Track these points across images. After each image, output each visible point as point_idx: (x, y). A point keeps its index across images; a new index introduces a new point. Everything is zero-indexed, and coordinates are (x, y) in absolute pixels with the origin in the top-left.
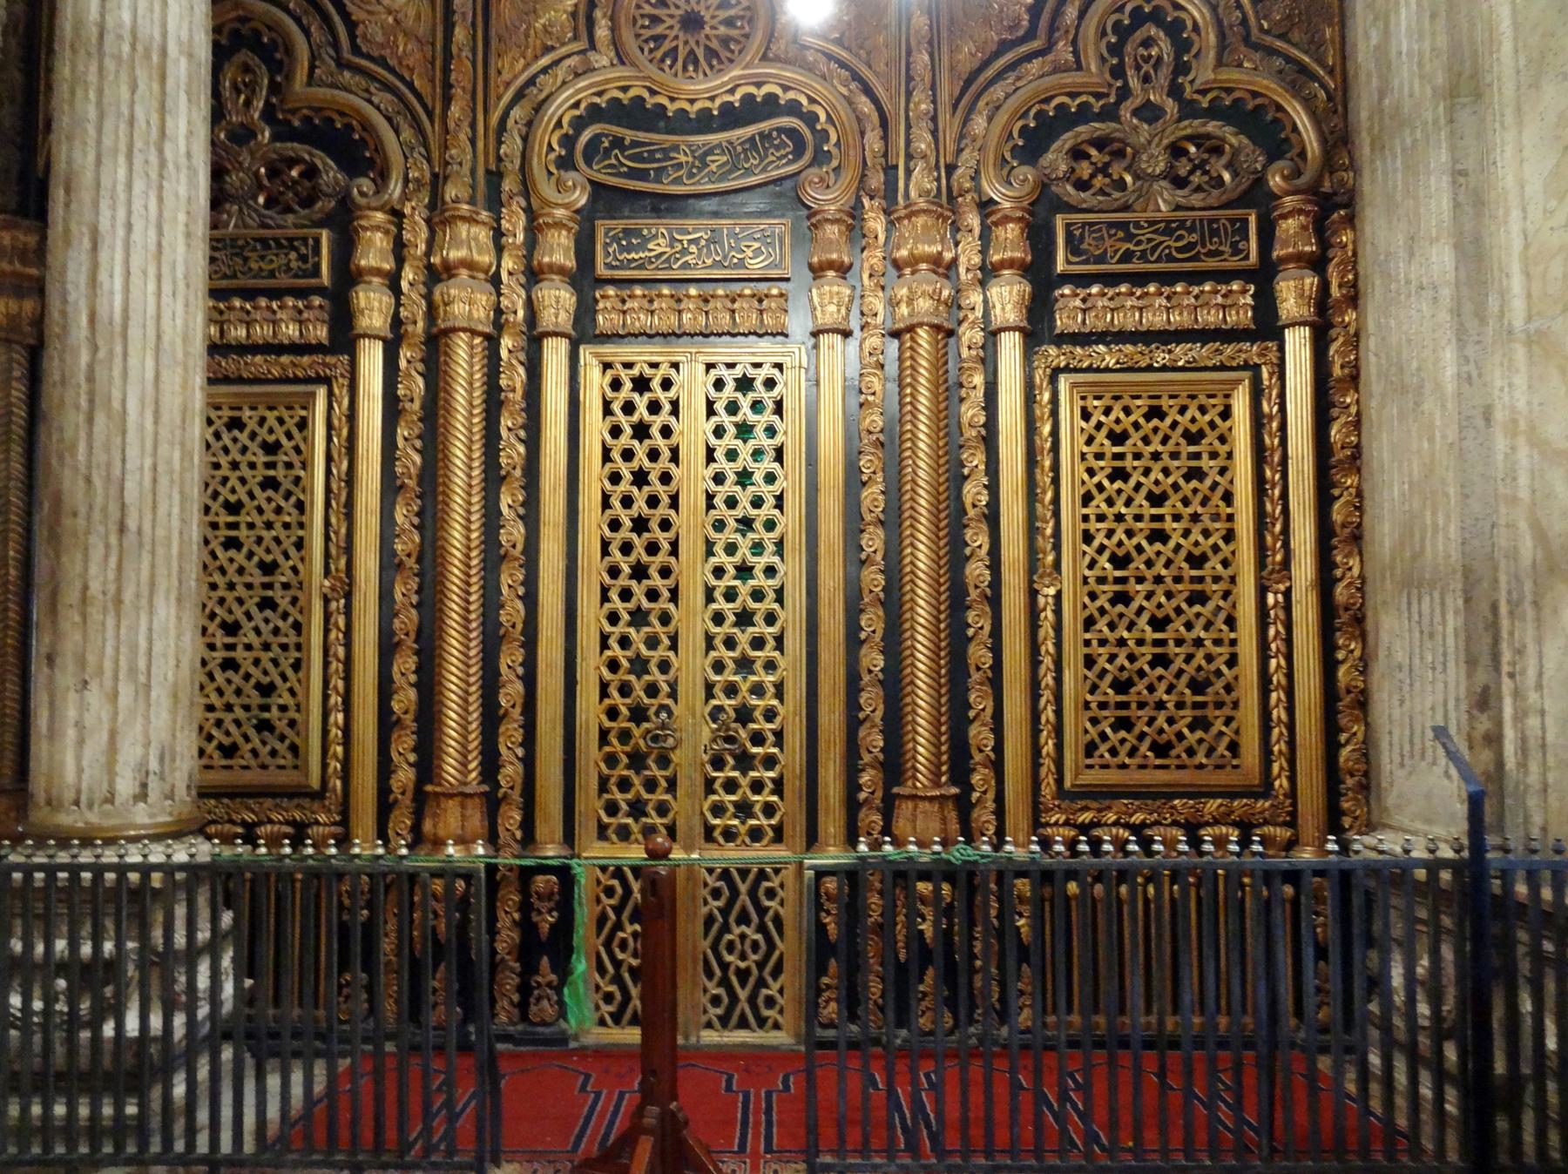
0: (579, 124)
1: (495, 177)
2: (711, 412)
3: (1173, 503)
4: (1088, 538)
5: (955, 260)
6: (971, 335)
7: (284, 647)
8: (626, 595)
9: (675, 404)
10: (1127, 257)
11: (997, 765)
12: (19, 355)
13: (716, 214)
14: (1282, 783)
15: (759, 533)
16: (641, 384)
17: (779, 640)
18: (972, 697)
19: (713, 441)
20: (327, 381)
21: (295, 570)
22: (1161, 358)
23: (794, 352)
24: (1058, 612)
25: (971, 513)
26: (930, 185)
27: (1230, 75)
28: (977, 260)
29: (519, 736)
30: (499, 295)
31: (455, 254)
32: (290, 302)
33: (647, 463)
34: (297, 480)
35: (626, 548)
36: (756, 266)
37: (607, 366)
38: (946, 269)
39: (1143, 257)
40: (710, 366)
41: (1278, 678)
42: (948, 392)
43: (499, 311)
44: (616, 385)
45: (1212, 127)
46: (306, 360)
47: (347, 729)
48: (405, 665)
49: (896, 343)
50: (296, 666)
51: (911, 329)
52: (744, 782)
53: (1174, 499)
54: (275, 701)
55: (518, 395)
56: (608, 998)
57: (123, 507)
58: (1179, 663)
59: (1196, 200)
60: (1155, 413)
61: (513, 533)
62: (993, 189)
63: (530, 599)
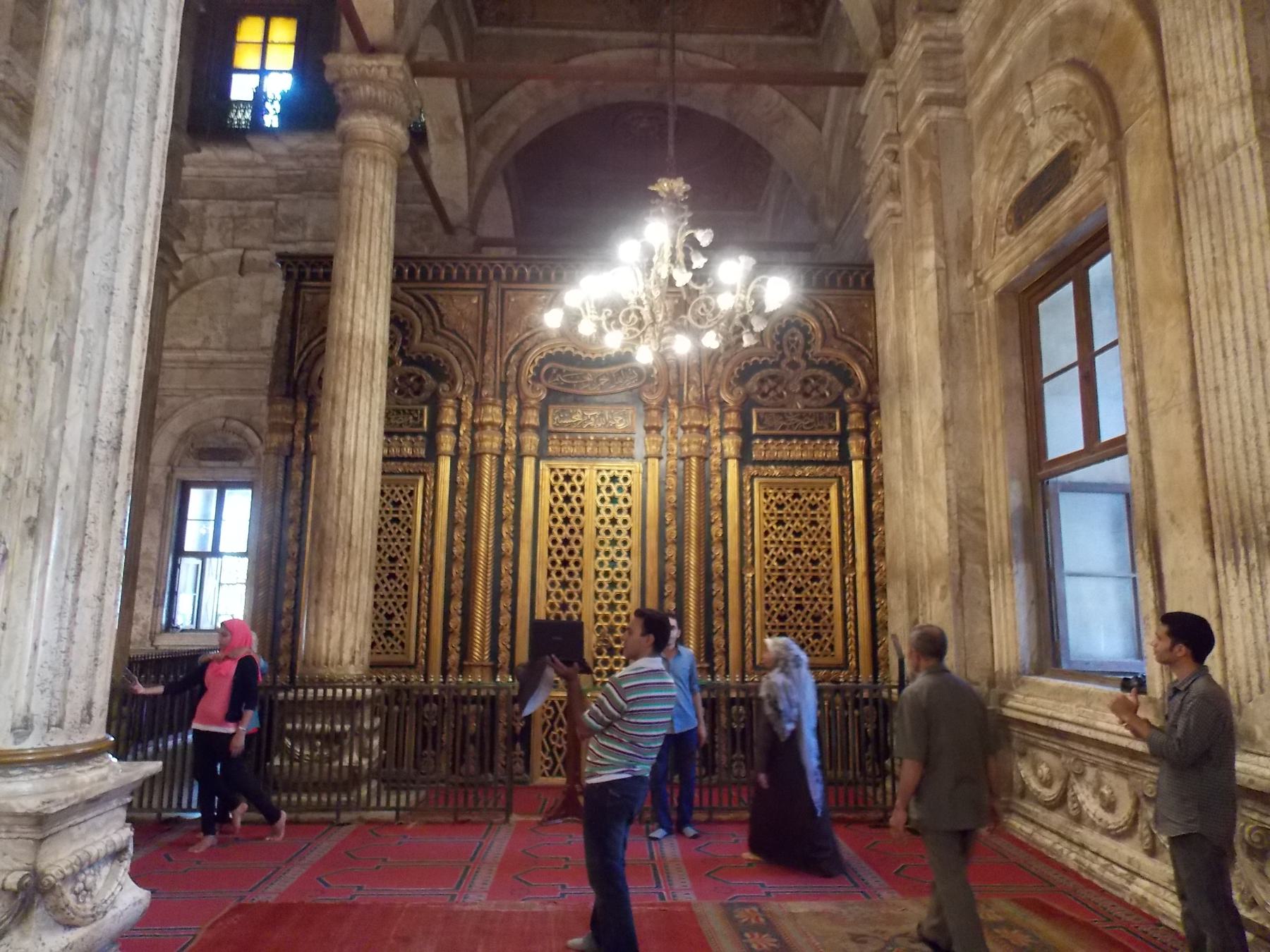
0: (542, 362)
1: (504, 384)
2: (599, 491)
3: (805, 536)
4: (767, 551)
5: (708, 427)
6: (715, 460)
7: (399, 597)
8: (559, 574)
9: (583, 487)
10: (783, 428)
11: (726, 653)
12: (282, 461)
13: (603, 403)
14: (853, 663)
15: (620, 546)
16: (568, 478)
17: (628, 595)
18: (715, 623)
19: (599, 504)
20: (425, 474)
21: (405, 561)
22: (798, 472)
23: (637, 466)
24: (753, 584)
25: (715, 539)
26: (697, 395)
27: (827, 351)
28: (718, 427)
29: (508, 639)
30: (504, 436)
31: (488, 419)
32: (408, 438)
33: (570, 514)
34: (408, 519)
35: (559, 552)
36: (621, 426)
37: (552, 470)
38: (703, 430)
39: (791, 428)
40: (599, 471)
41: (851, 616)
42: (704, 485)
43: (504, 444)
44: (556, 478)
45: (821, 372)
46: (414, 464)
47: (428, 635)
48: (457, 605)
49: (681, 464)
50: (405, 606)
51: (689, 457)
52: (612, 661)
53: (805, 535)
54: (394, 622)
55: (511, 483)
56: (547, 763)
57: (351, 537)
58: (807, 608)
59: (814, 403)
60: (796, 496)
61: (508, 545)
62: (725, 396)
63: (515, 575)
